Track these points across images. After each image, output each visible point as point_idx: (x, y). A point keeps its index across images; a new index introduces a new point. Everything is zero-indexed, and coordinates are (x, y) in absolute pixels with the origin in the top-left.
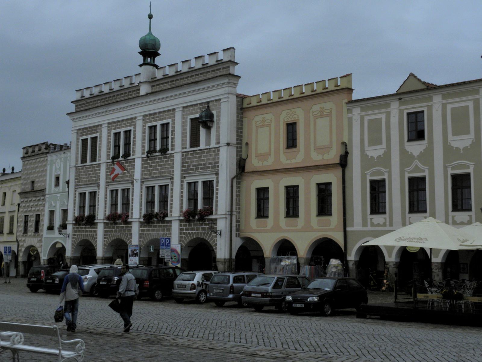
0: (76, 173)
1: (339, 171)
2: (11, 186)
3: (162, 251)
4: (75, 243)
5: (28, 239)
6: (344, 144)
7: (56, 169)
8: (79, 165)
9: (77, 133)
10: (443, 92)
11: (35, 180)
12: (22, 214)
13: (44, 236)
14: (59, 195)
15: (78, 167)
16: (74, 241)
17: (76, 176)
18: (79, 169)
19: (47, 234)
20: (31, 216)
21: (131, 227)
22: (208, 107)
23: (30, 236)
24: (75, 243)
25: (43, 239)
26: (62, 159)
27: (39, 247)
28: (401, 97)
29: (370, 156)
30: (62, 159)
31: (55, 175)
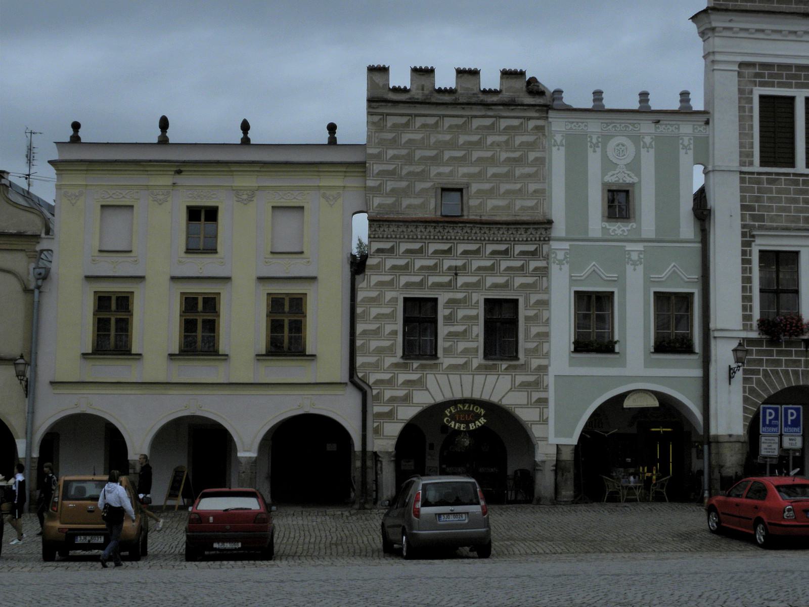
0: (742, 190)
2: (259, 188)
4: (758, 396)
5: (443, 379)
7: (607, 165)
8: (757, 167)
9: (740, 75)
11: (468, 186)
12: (389, 295)
13: (553, 371)
14: (640, 247)
15: (753, 173)
16: (752, 390)
17: (743, 199)
18: (759, 182)
19: (648, 364)
20: (451, 302)
23: (454, 368)
24: (758, 396)
25: (550, 380)
26: (648, 140)
27: (521, 406)
30: (648, 140)
31: (604, 184)
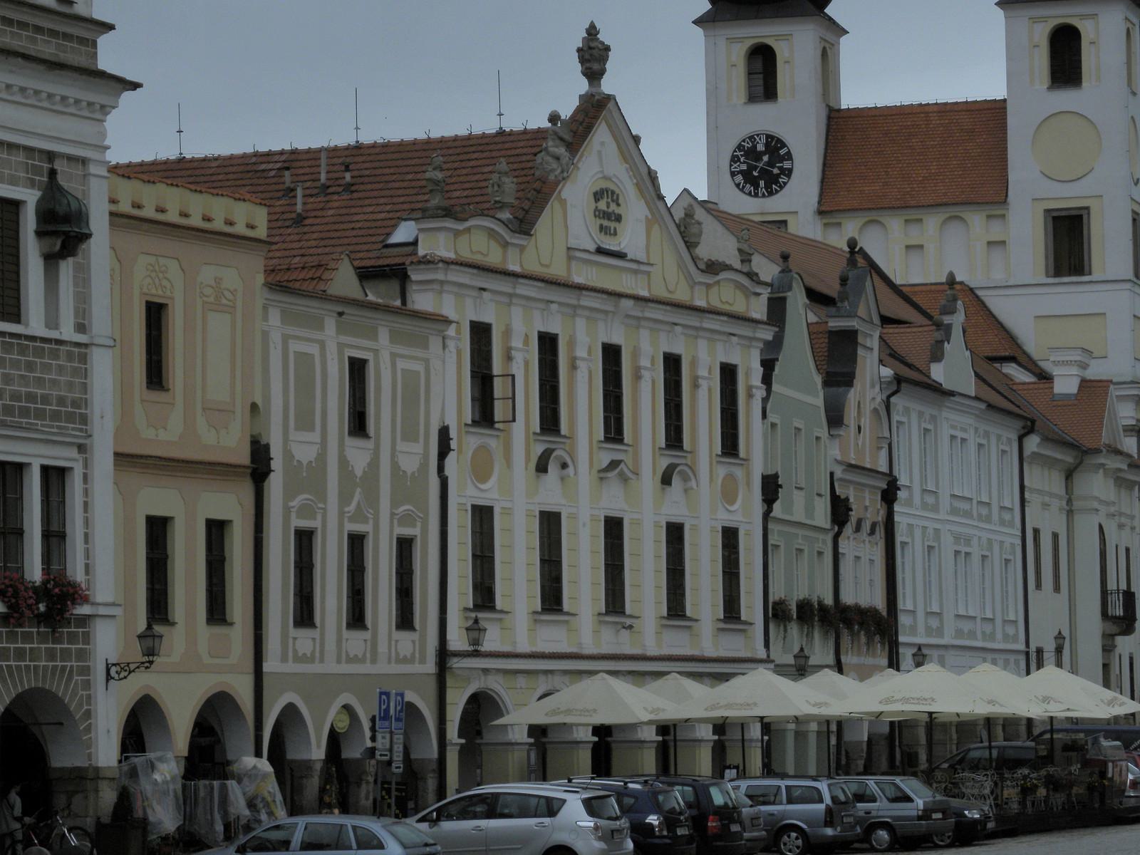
1: (246, 491)
3: (384, 738)
6: (254, 407)
10: (395, 325)
21: (87, 638)
22: (53, 173)
28: (346, 310)
29: (297, 458)
